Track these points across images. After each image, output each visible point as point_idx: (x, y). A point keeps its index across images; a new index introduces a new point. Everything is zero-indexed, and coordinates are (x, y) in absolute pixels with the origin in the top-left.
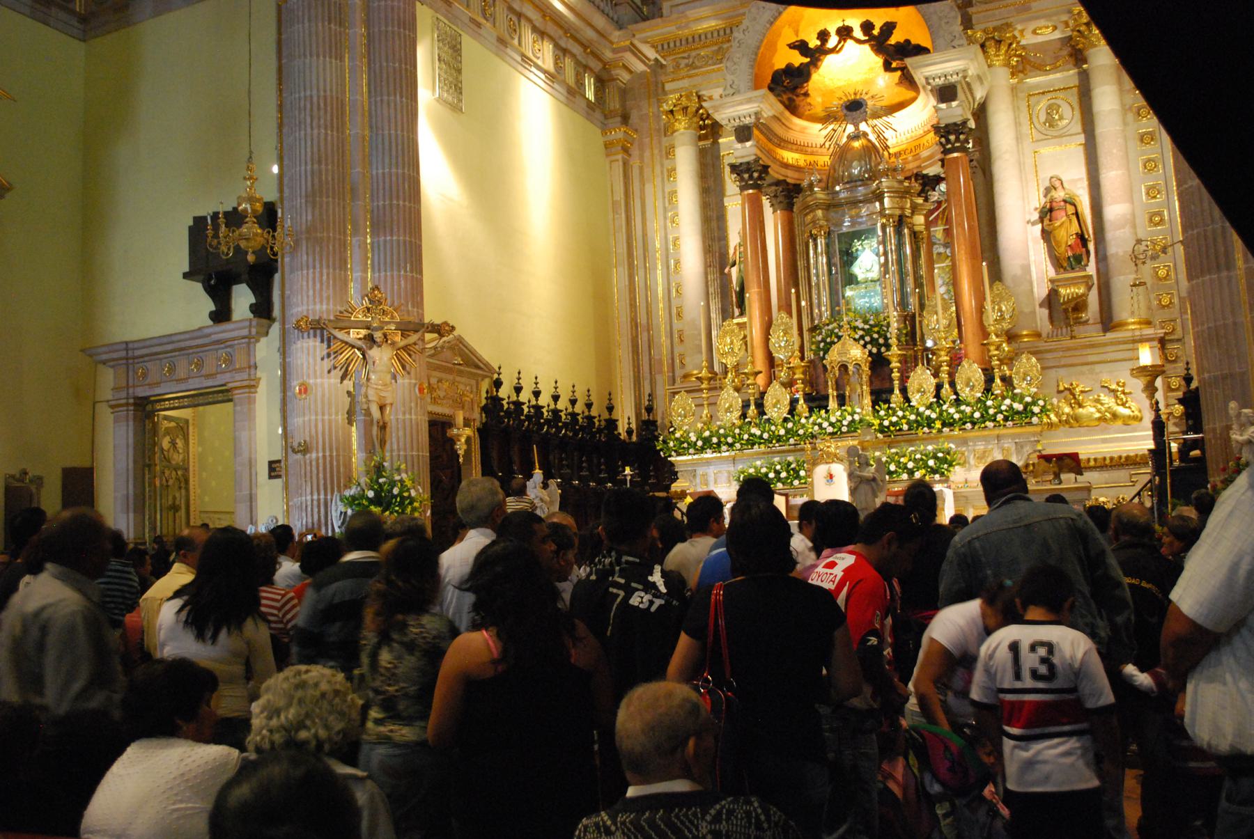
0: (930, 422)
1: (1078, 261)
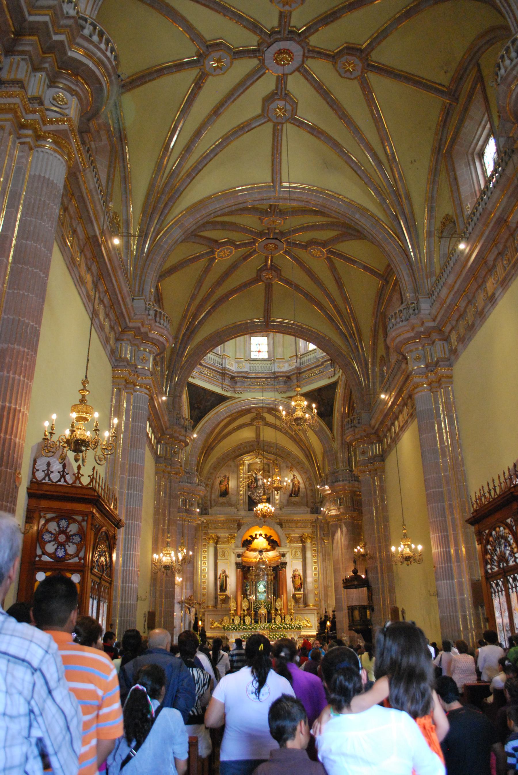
0: (281, 628)
1: (299, 589)
